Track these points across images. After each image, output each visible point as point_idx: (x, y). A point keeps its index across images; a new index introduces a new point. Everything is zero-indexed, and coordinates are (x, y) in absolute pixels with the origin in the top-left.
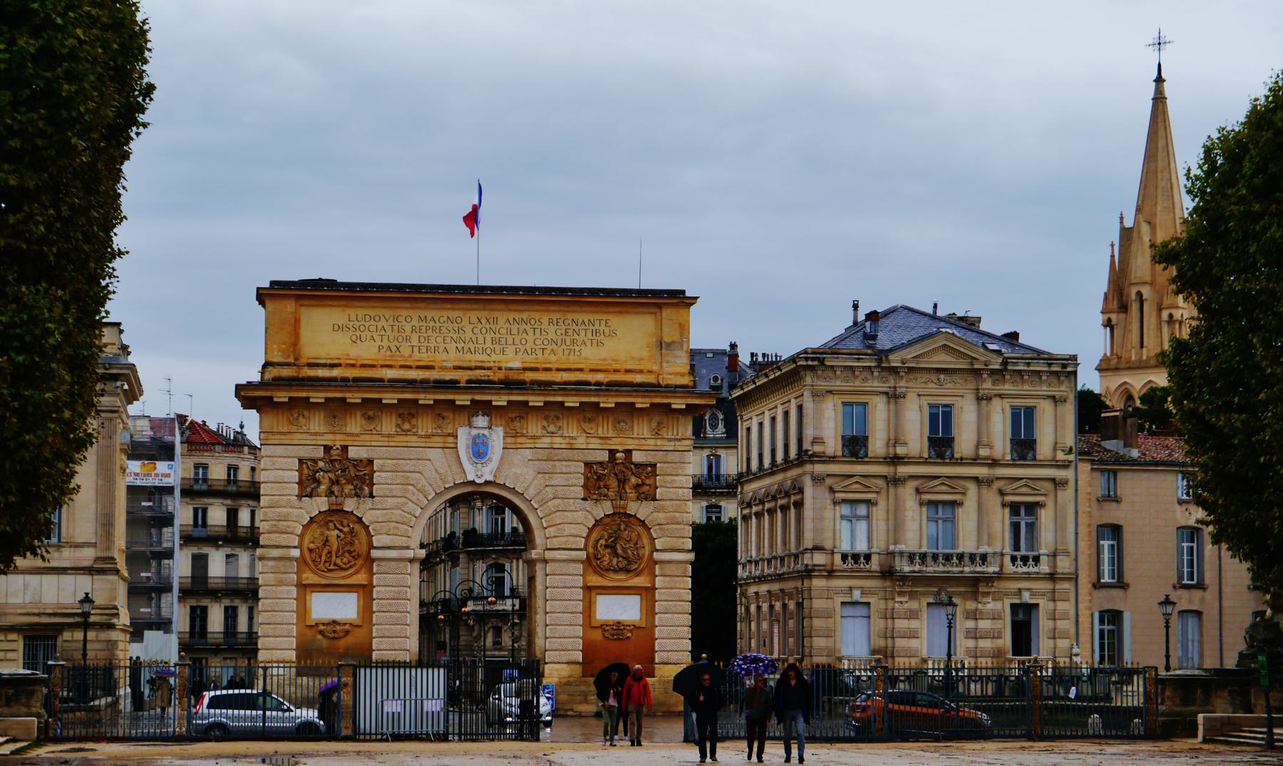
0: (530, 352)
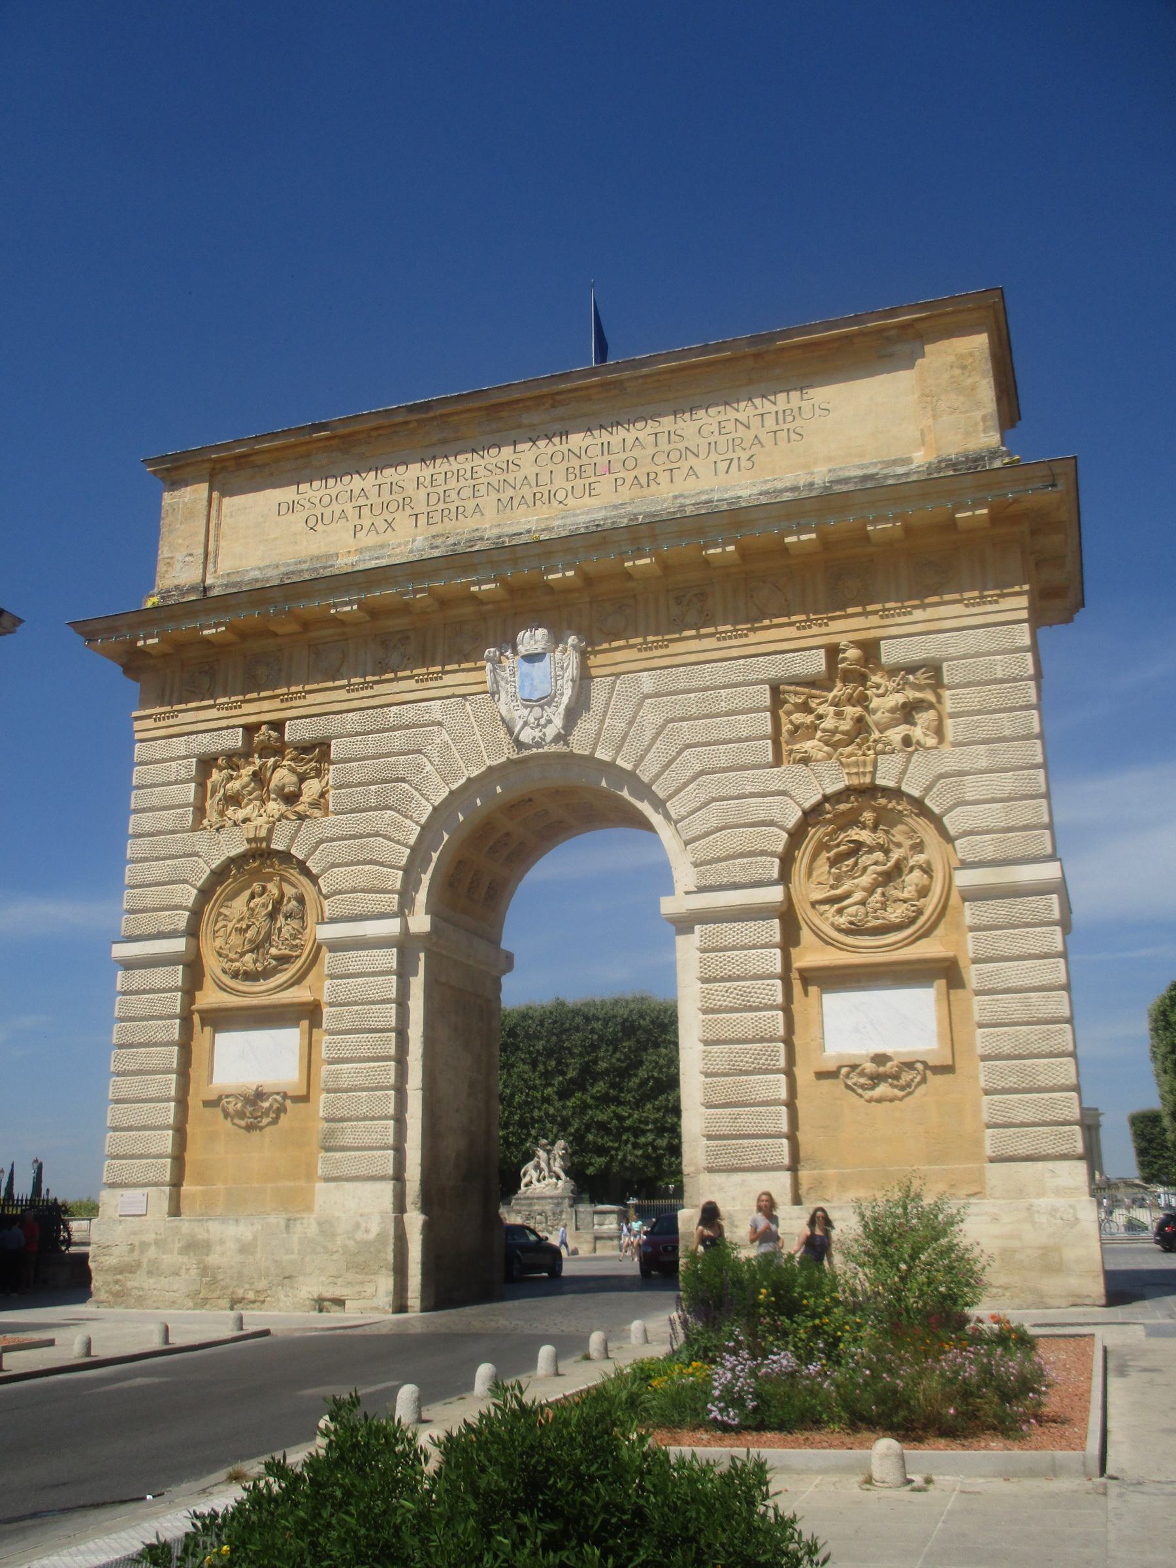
0: (644, 481)
